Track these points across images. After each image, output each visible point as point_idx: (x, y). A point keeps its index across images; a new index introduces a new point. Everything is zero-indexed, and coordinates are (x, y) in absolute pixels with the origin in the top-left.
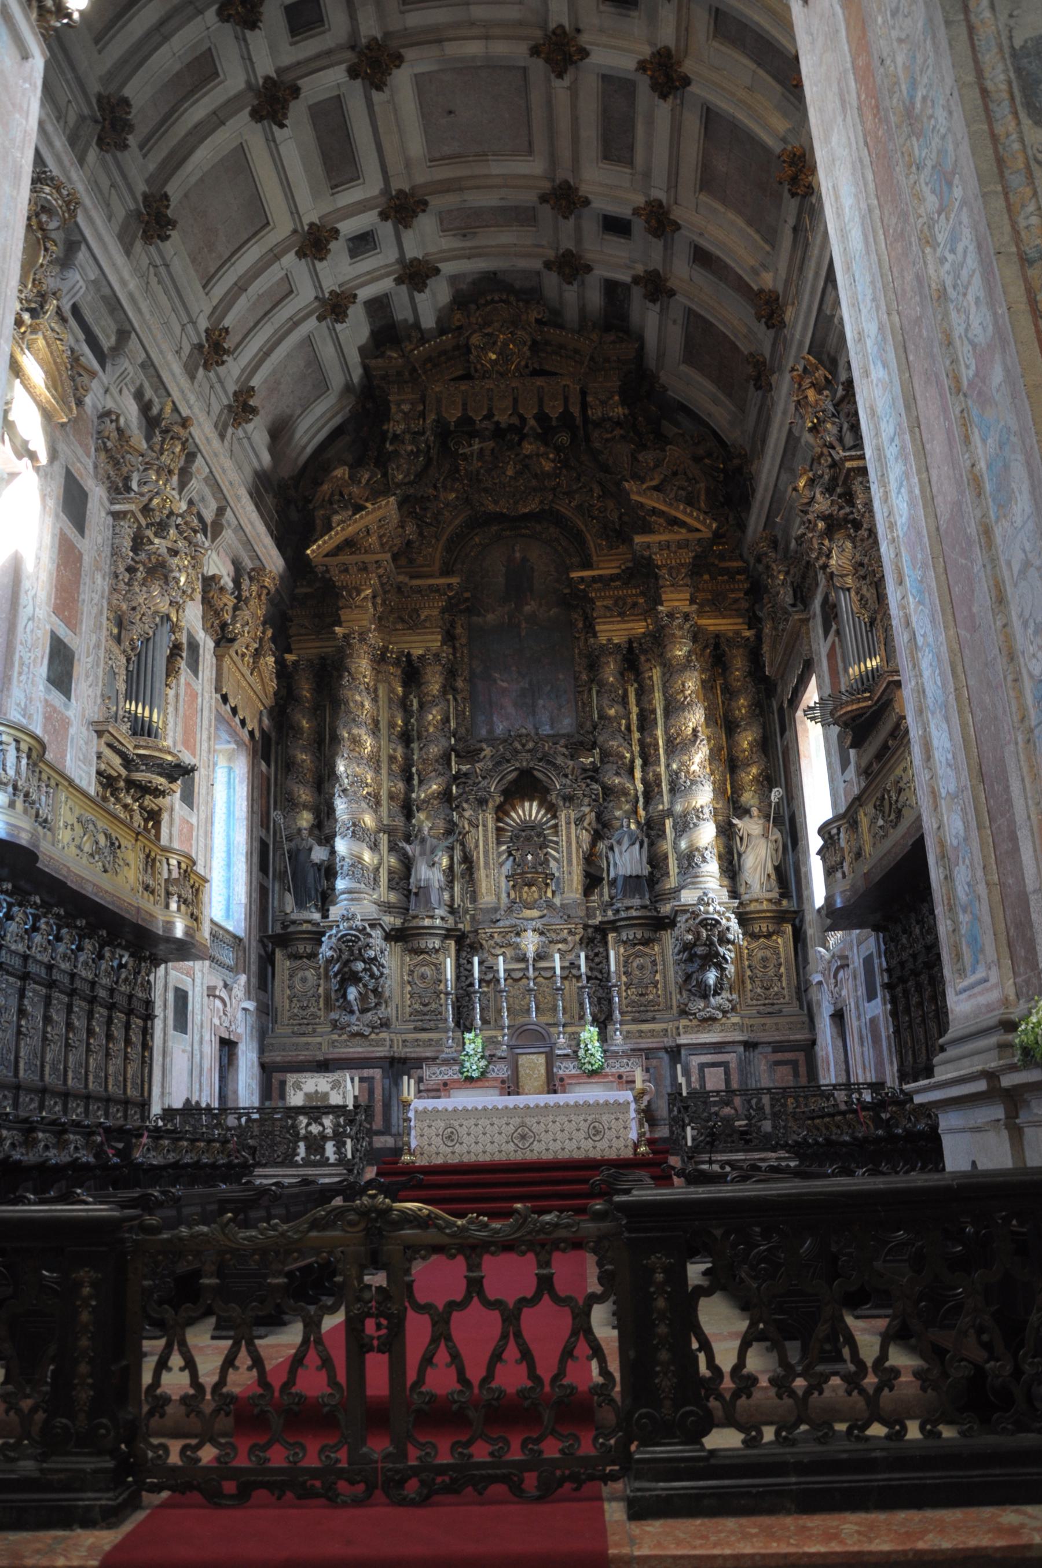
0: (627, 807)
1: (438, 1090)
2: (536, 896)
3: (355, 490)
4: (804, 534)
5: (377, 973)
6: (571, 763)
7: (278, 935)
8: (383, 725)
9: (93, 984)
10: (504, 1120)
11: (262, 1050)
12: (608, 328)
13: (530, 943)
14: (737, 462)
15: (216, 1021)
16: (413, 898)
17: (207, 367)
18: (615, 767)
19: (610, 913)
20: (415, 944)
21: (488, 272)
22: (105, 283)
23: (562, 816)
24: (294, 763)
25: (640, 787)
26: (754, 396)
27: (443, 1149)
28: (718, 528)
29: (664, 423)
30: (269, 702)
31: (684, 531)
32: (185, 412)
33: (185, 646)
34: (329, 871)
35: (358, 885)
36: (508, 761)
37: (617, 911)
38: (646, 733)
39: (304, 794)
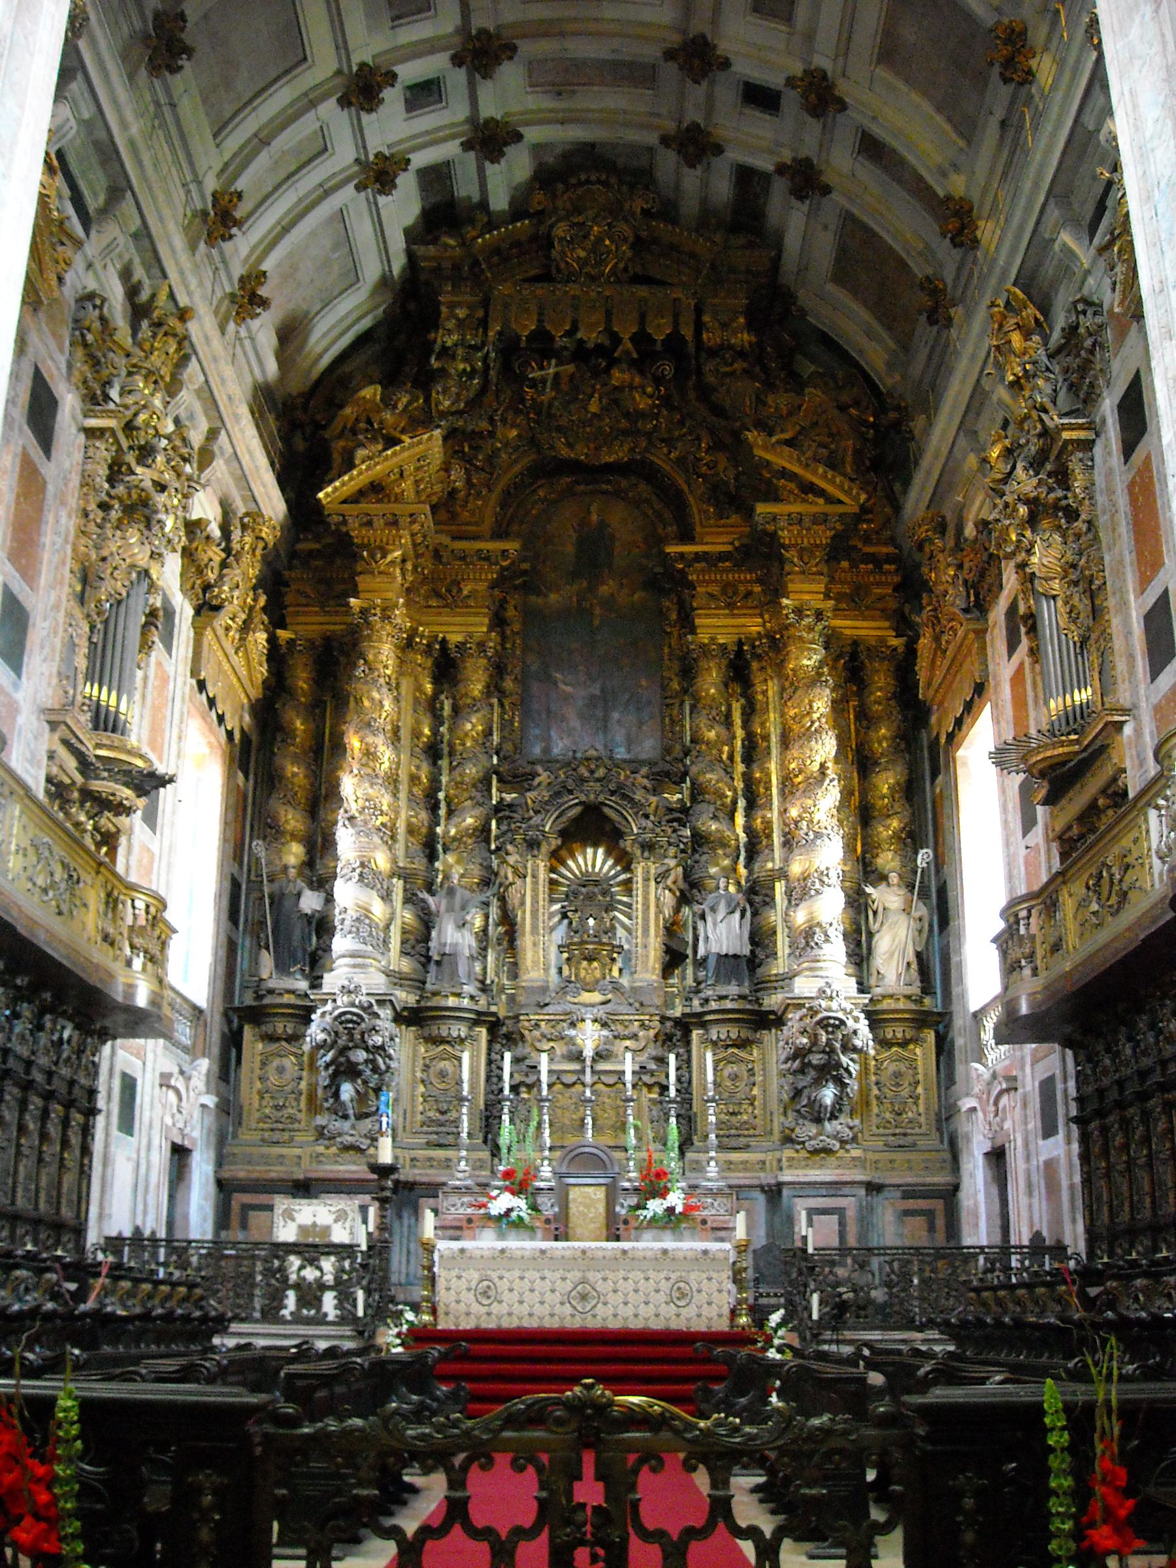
0: (726, 862)
1: (460, 1228)
2: (598, 974)
3: (388, 416)
4: (998, 521)
5: (383, 1067)
6: (654, 800)
7: (250, 1007)
8: (405, 733)
9: (29, 1064)
10: (558, 1275)
11: (220, 1162)
12: (734, 228)
13: (589, 1037)
14: (893, 415)
15: (168, 1121)
16: (432, 967)
17: (211, 240)
18: (712, 808)
19: (696, 1002)
20: (435, 1032)
21: (585, 144)
22: (100, 124)
23: (639, 870)
24: (281, 778)
25: (743, 838)
26: (925, 333)
27: (476, 1308)
28: (868, 500)
29: (799, 357)
30: (256, 693)
31: (821, 501)
32: (183, 301)
33: (161, 613)
34: (323, 926)
35: (363, 947)
36: (570, 792)
37: (707, 1001)
38: (755, 766)
39: (292, 819)
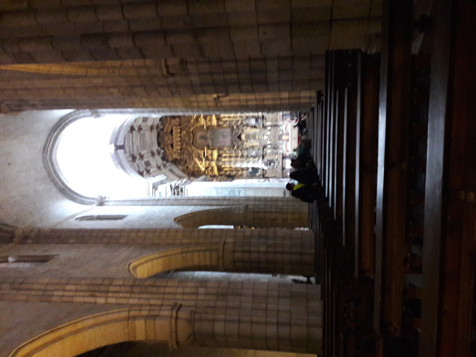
13: (266, 137)
34: (253, 168)
39: (240, 173)
